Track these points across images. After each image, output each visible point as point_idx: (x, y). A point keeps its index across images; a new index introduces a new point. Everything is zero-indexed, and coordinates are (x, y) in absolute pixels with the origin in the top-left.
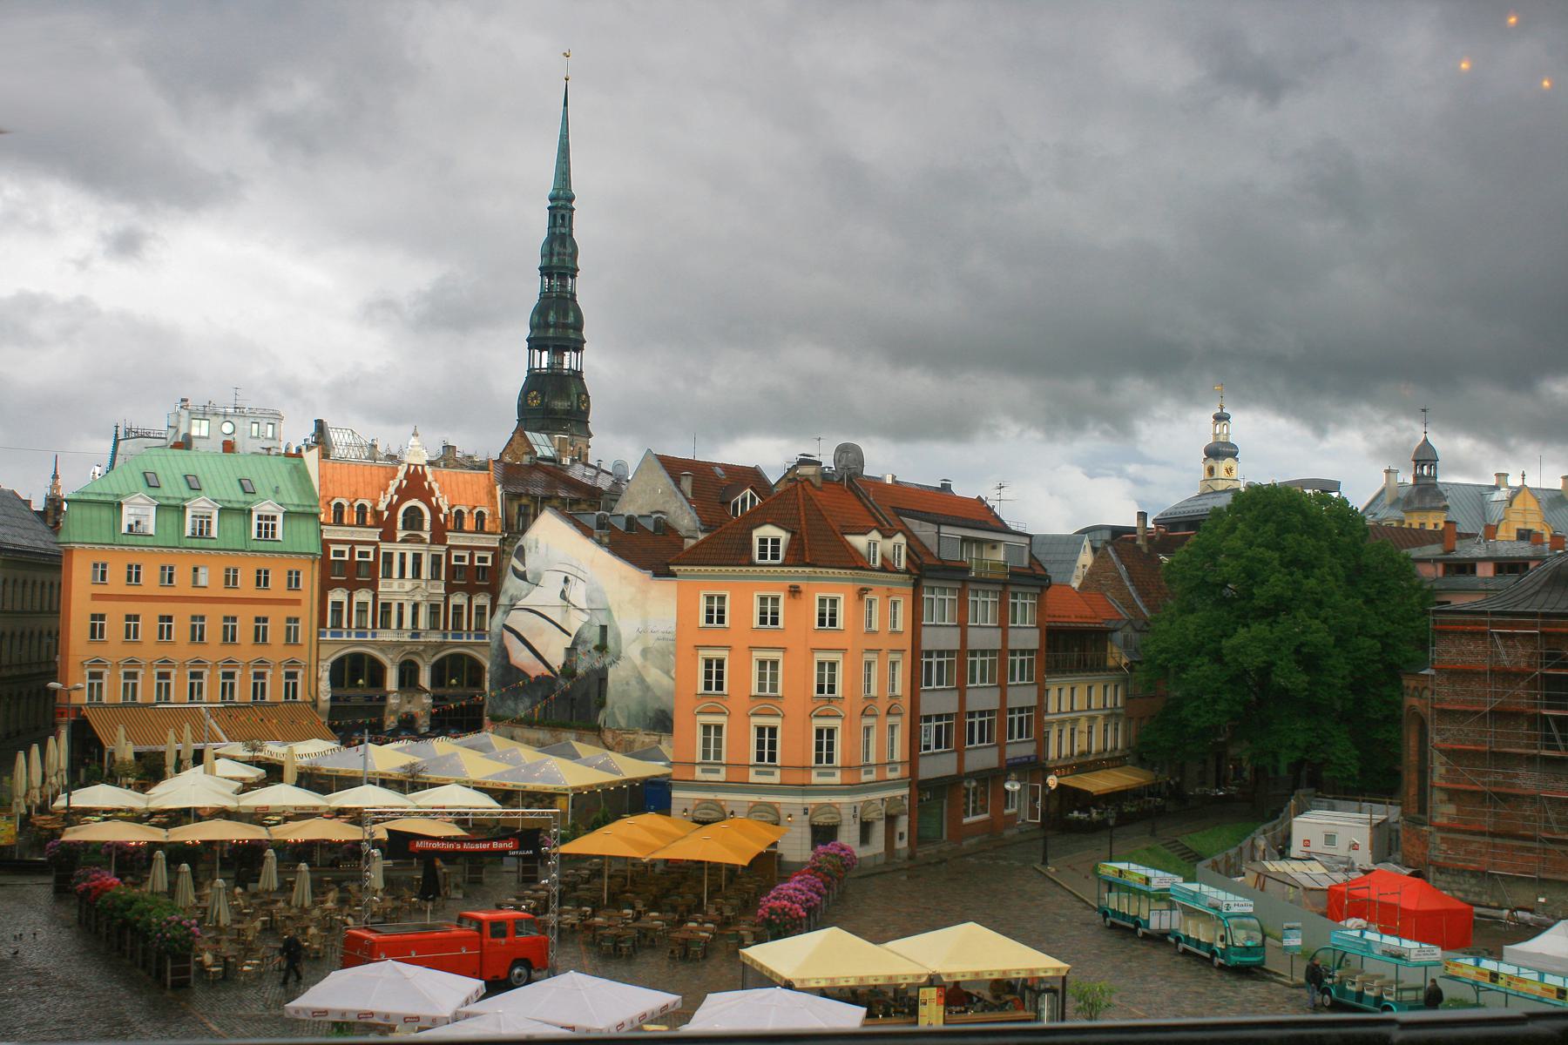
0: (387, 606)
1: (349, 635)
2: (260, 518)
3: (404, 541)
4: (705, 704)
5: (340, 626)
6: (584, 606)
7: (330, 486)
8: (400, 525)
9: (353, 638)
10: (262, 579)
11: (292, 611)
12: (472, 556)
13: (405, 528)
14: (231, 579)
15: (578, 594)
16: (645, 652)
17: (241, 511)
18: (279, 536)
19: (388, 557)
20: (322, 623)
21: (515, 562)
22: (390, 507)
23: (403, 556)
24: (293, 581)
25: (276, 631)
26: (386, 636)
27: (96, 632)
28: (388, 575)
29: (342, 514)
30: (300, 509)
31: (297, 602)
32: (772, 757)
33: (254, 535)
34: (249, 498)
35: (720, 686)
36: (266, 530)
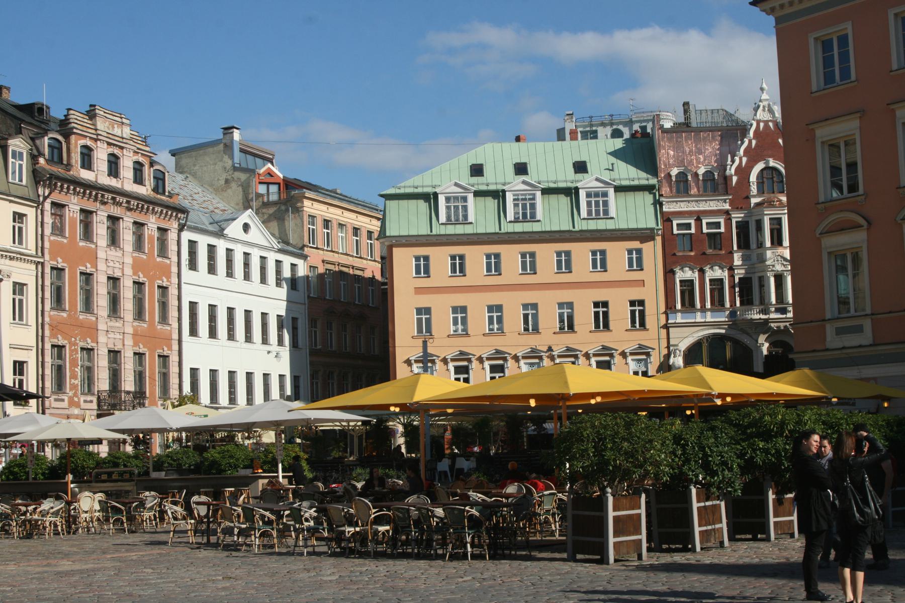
2: (589, 195)
5: (692, 304)
8: (754, 189)
13: (761, 192)
22: (739, 170)
25: (620, 314)
27: (425, 327)
30: (636, 183)
31: (642, 283)
33: (584, 214)
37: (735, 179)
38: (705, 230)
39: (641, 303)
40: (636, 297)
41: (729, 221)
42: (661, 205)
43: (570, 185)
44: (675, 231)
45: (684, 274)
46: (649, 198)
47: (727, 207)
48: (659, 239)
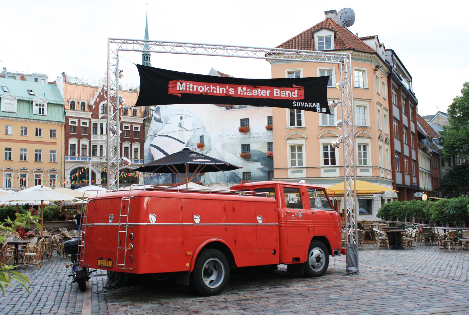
0: (95, 147)
1: (79, 159)
3: (102, 118)
4: (292, 133)
6: (191, 128)
7: (69, 94)
9: (80, 160)
10: (38, 133)
11: (53, 148)
12: (132, 126)
14: (24, 132)
15: (187, 123)
16: (223, 146)
17: (28, 102)
18: (46, 113)
19: (95, 125)
20: (66, 153)
21: (155, 115)
22: (95, 103)
23: (102, 125)
24: (53, 134)
25: (45, 157)
26: (96, 159)
28: (95, 133)
29: (74, 105)
30: (56, 103)
31: (55, 144)
32: (333, 162)
34: (31, 97)
35: (299, 123)
36: (41, 112)
37: (94, 106)
38: (81, 125)
39: (54, 152)
40: (53, 149)
41: (90, 122)
42: (65, 112)
43: (28, 99)
44: (70, 124)
45: (73, 141)
46: (60, 109)
47: (90, 117)
48: (63, 127)
